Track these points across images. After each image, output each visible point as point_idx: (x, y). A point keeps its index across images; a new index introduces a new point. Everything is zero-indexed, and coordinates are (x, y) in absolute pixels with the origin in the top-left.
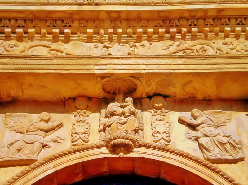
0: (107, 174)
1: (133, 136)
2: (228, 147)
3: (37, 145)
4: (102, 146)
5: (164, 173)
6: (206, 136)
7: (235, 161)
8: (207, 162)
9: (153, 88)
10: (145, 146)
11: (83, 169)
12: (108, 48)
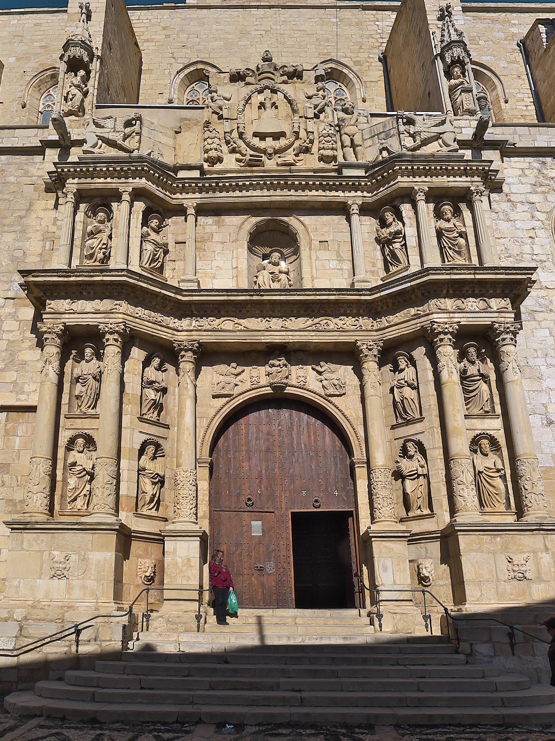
1: (285, 381)
2: (338, 387)
3: (232, 384)
4: (268, 386)
6: (326, 380)
7: (340, 395)
10: (292, 386)
12: (269, 321)
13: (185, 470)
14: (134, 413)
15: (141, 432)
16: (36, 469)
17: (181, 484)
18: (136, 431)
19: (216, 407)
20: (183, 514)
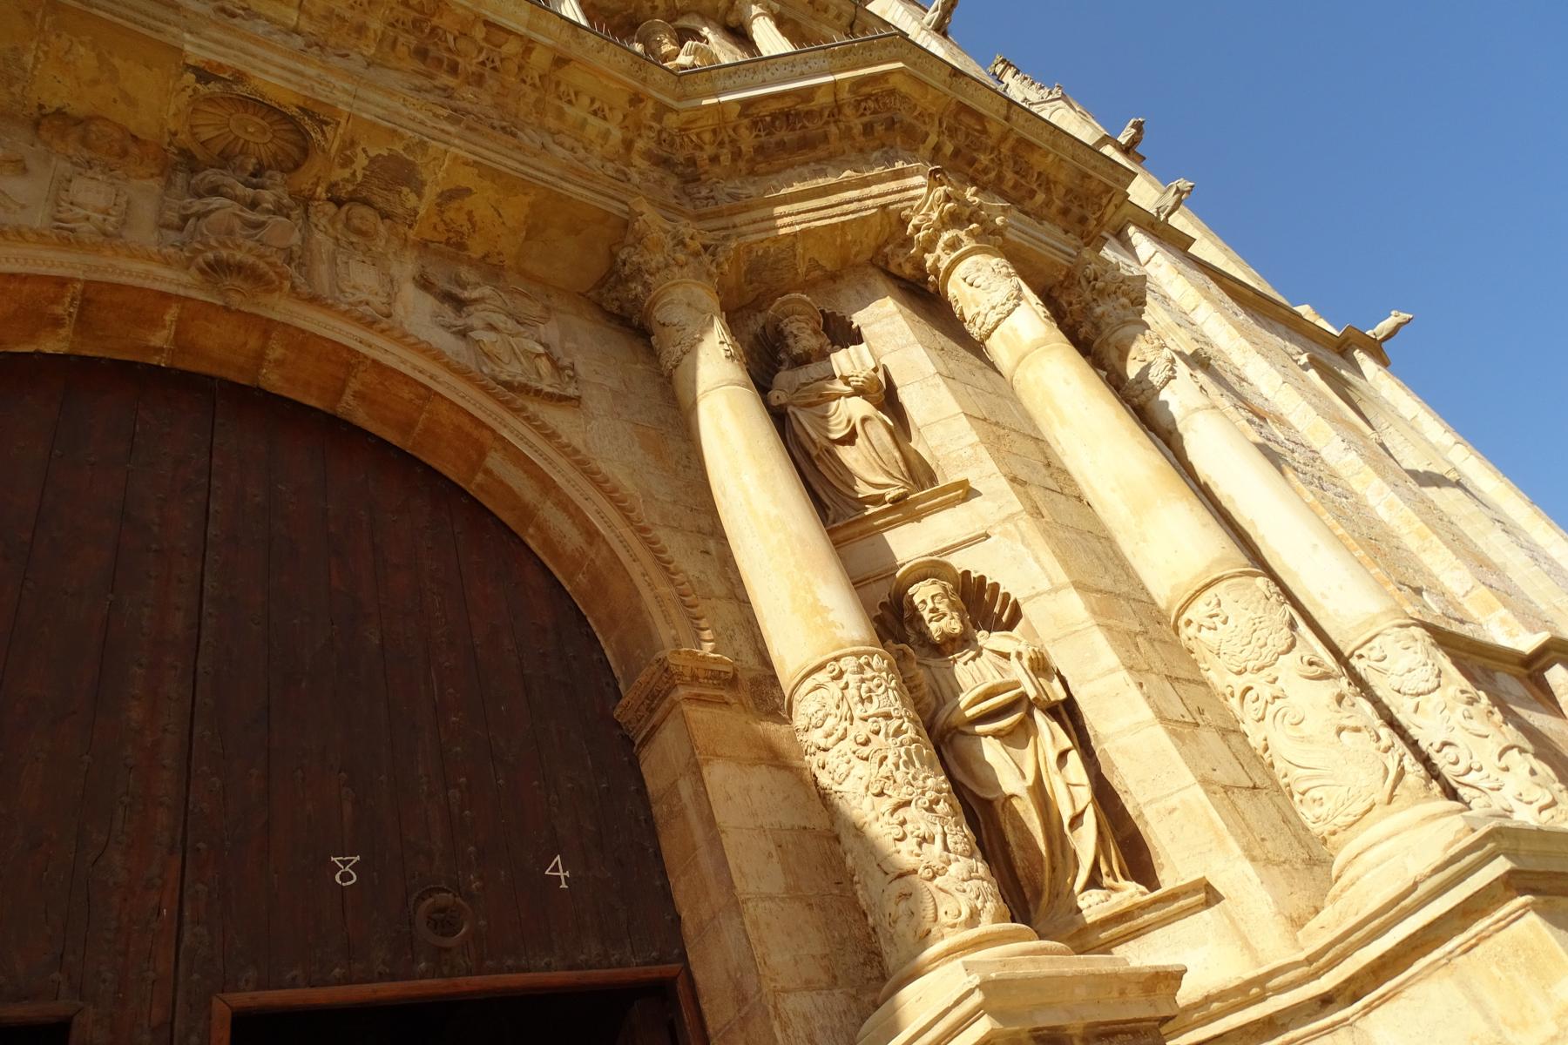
0: (161, 361)
5: (356, 395)
8: (493, 384)
9: (354, 175)
11: (81, 309)
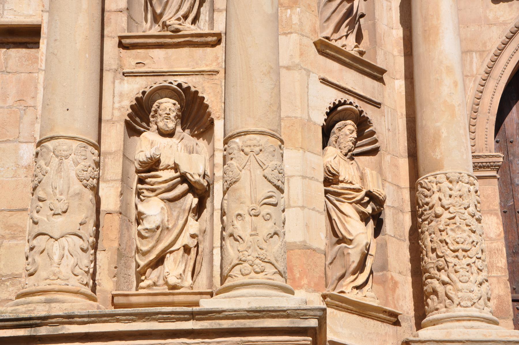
13: (454, 176)
14: (307, 28)
15: (324, 81)
16: (59, 171)
17: (446, 215)
18: (314, 79)
19: (504, 23)
20: (462, 299)
